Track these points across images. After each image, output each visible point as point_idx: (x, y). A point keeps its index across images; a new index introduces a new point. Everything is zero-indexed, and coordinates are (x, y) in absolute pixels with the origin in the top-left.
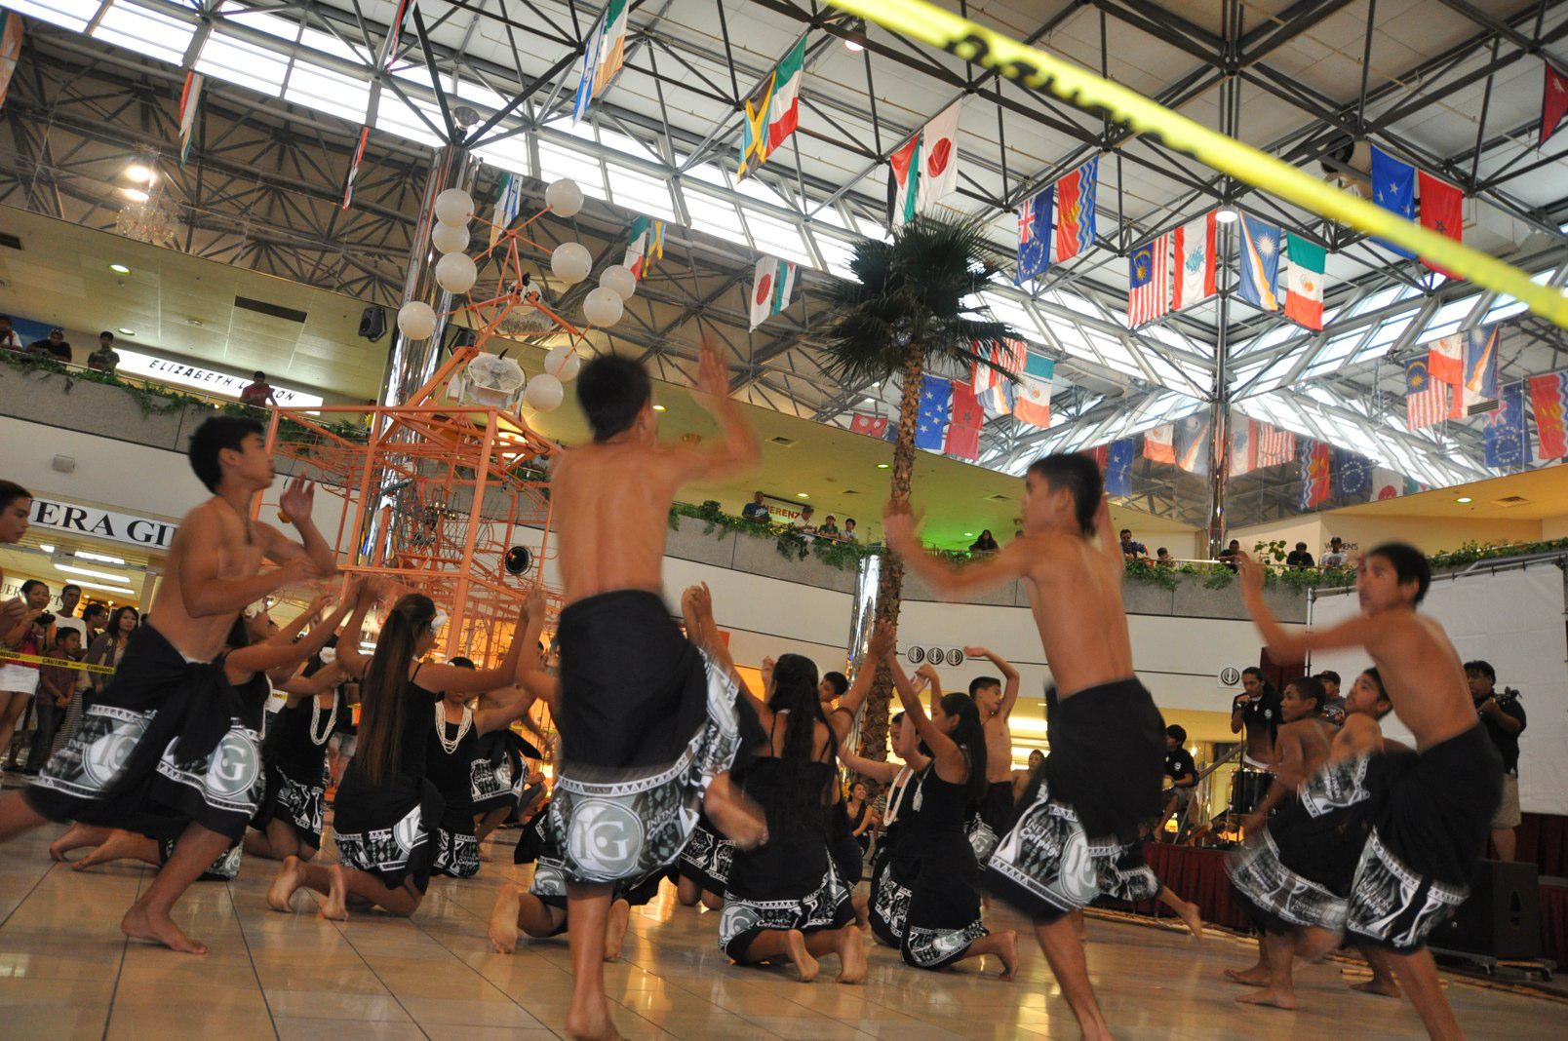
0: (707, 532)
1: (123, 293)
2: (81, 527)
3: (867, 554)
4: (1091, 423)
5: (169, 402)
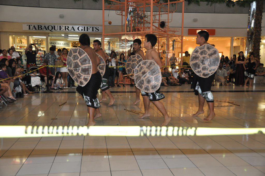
0: (207, 5)
2: (68, 30)
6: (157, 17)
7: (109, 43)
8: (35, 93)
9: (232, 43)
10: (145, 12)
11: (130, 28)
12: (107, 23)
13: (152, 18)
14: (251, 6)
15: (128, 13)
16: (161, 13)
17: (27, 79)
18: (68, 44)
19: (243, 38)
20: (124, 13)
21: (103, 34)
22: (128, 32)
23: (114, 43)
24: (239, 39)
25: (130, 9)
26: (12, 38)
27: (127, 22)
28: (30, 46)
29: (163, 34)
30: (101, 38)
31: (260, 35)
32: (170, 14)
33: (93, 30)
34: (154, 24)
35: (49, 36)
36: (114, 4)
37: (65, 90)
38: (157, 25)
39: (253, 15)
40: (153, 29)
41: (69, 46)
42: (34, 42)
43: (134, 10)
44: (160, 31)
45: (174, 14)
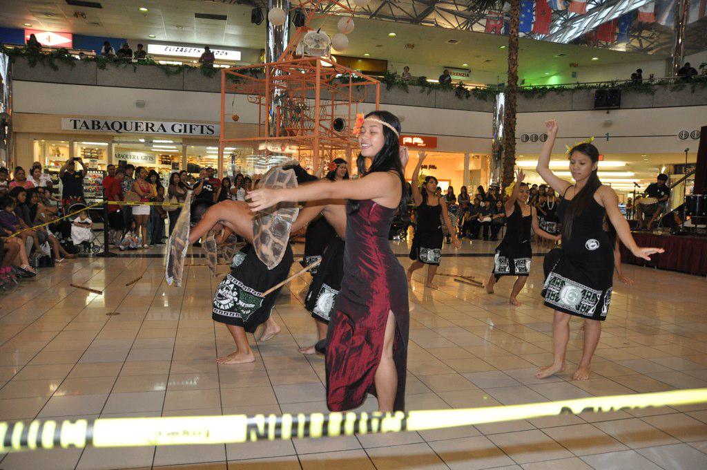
0: (422, 91)
1: (146, 20)
2: (153, 130)
3: (498, 93)
4: (608, 7)
6: (329, 110)
7: (233, 157)
8: (80, 256)
9: (466, 164)
11: (275, 129)
13: (319, 111)
15: (271, 98)
17: (64, 229)
18: (152, 159)
19: (485, 156)
20: (264, 100)
21: (222, 139)
22: (271, 136)
23: (244, 157)
24: (478, 157)
25: (277, 92)
26: (40, 145)
27: (270, 118)
28: (73, 160)
29: (339, 143)
30: (219, 148)
31: (514, 152)
32: (353, 106)
33: (202, 132)
34: (322, 123)
35: (114, 142)
36: (245, 83)
37: (140, 252)
38: (328, 125)
39: (500, 116)
40: (320, 132)
41: (155, 163)
42: (83, 153)
43: (285, 95)
44: (334, 136)
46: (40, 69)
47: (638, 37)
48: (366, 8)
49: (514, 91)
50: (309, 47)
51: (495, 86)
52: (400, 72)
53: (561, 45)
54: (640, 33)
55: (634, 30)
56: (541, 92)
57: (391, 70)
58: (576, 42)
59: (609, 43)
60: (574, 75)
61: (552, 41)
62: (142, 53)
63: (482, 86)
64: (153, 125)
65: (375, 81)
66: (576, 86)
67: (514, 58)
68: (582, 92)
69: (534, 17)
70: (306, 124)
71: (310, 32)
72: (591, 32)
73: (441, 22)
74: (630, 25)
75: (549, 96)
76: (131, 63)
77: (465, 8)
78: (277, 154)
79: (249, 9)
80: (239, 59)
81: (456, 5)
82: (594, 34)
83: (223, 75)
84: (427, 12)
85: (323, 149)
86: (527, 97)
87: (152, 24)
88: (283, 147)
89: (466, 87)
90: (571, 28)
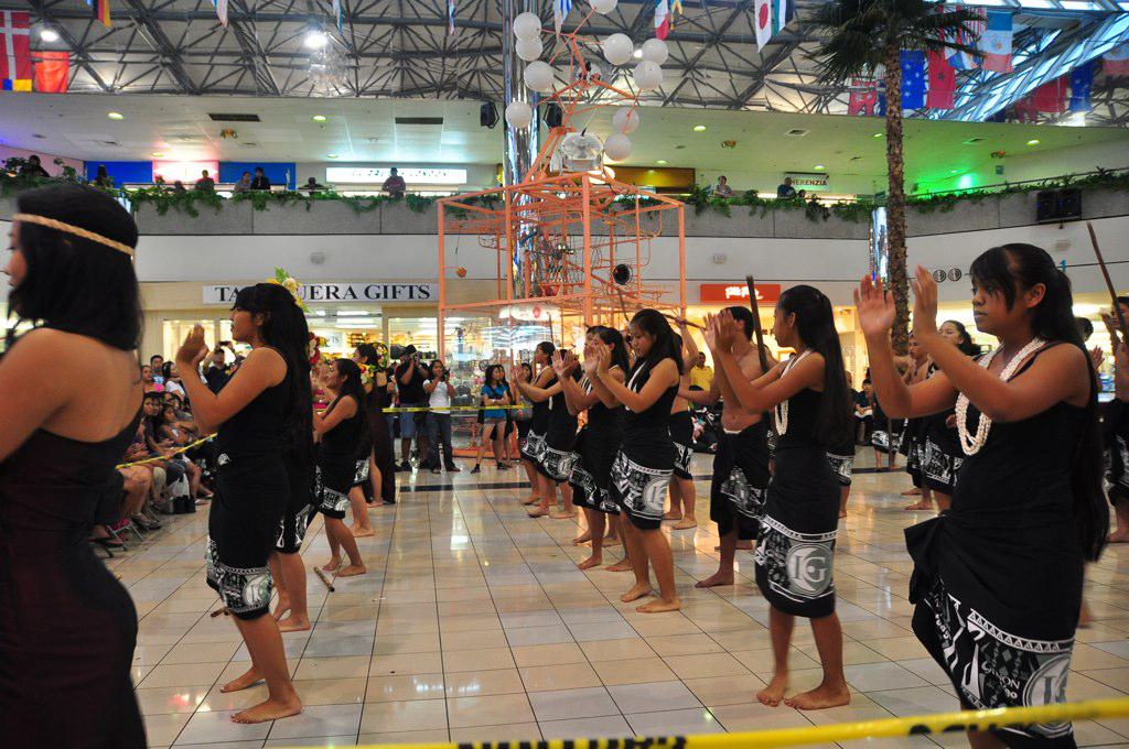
0: (751, 214)
1: (323, 133)
3: (875, 207)
5: (370, 202)
7: (460, 332)
10: (568, 238)
12: (452, 275)
14: (872, 221)
16: (614, 240)
20: (504, 242)
21: (441, 306)
22: (518, 297)
24: (848, 311)
25: (525, 228)
27: (515, 268)
32: (644, 243)
33: (411, 296)
34: (596, 272)
38: (605, 274)
41: (340, 346)
45: (656, 240)
46: (174, 217)
47: (1105, 101)
48: (658, 90)
49: (900, 204)
50: (570, 158)
51: (870, 196)
52: (715, 184)
53: (974, 124)
54: (1111, 93)
55: (1100, 90)
56: (944, 203)
57: (701, 183)
58: (999, 117)
59: (1057, 114)
60: (1000, 171)
61: (958, 119)
62: (312, 184)
63: (849, 199)
64: (337, 289)
65: (676, 203)
66: (1004, 187)
67: (897, 151)
68: (1014, 198)
69: (927, 85)
70: (571, 275)
71: (569, 135)
72: (1023, 100)
73: (777, 103)
74: (1090, 81)
75: (959, 208)
76: (301, 198)
77: (813, 79)
78: (527, 323)
79: (476, 106)
80: (465, 181)
81: (799, 74)
82: (1028, 102)
83: (441, 211)
84: (753, 90)
85: (598, 312)
86: (923, 212)
87: (336, 137)
88: (537, 309)
89: (821, 203)
90: (991, 97)
